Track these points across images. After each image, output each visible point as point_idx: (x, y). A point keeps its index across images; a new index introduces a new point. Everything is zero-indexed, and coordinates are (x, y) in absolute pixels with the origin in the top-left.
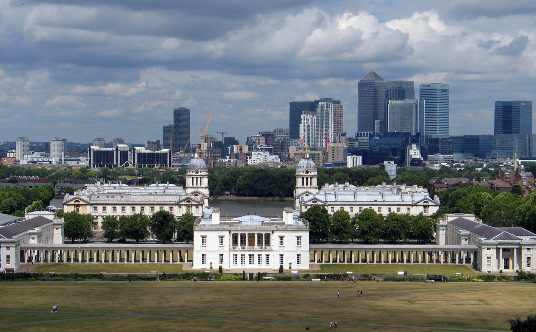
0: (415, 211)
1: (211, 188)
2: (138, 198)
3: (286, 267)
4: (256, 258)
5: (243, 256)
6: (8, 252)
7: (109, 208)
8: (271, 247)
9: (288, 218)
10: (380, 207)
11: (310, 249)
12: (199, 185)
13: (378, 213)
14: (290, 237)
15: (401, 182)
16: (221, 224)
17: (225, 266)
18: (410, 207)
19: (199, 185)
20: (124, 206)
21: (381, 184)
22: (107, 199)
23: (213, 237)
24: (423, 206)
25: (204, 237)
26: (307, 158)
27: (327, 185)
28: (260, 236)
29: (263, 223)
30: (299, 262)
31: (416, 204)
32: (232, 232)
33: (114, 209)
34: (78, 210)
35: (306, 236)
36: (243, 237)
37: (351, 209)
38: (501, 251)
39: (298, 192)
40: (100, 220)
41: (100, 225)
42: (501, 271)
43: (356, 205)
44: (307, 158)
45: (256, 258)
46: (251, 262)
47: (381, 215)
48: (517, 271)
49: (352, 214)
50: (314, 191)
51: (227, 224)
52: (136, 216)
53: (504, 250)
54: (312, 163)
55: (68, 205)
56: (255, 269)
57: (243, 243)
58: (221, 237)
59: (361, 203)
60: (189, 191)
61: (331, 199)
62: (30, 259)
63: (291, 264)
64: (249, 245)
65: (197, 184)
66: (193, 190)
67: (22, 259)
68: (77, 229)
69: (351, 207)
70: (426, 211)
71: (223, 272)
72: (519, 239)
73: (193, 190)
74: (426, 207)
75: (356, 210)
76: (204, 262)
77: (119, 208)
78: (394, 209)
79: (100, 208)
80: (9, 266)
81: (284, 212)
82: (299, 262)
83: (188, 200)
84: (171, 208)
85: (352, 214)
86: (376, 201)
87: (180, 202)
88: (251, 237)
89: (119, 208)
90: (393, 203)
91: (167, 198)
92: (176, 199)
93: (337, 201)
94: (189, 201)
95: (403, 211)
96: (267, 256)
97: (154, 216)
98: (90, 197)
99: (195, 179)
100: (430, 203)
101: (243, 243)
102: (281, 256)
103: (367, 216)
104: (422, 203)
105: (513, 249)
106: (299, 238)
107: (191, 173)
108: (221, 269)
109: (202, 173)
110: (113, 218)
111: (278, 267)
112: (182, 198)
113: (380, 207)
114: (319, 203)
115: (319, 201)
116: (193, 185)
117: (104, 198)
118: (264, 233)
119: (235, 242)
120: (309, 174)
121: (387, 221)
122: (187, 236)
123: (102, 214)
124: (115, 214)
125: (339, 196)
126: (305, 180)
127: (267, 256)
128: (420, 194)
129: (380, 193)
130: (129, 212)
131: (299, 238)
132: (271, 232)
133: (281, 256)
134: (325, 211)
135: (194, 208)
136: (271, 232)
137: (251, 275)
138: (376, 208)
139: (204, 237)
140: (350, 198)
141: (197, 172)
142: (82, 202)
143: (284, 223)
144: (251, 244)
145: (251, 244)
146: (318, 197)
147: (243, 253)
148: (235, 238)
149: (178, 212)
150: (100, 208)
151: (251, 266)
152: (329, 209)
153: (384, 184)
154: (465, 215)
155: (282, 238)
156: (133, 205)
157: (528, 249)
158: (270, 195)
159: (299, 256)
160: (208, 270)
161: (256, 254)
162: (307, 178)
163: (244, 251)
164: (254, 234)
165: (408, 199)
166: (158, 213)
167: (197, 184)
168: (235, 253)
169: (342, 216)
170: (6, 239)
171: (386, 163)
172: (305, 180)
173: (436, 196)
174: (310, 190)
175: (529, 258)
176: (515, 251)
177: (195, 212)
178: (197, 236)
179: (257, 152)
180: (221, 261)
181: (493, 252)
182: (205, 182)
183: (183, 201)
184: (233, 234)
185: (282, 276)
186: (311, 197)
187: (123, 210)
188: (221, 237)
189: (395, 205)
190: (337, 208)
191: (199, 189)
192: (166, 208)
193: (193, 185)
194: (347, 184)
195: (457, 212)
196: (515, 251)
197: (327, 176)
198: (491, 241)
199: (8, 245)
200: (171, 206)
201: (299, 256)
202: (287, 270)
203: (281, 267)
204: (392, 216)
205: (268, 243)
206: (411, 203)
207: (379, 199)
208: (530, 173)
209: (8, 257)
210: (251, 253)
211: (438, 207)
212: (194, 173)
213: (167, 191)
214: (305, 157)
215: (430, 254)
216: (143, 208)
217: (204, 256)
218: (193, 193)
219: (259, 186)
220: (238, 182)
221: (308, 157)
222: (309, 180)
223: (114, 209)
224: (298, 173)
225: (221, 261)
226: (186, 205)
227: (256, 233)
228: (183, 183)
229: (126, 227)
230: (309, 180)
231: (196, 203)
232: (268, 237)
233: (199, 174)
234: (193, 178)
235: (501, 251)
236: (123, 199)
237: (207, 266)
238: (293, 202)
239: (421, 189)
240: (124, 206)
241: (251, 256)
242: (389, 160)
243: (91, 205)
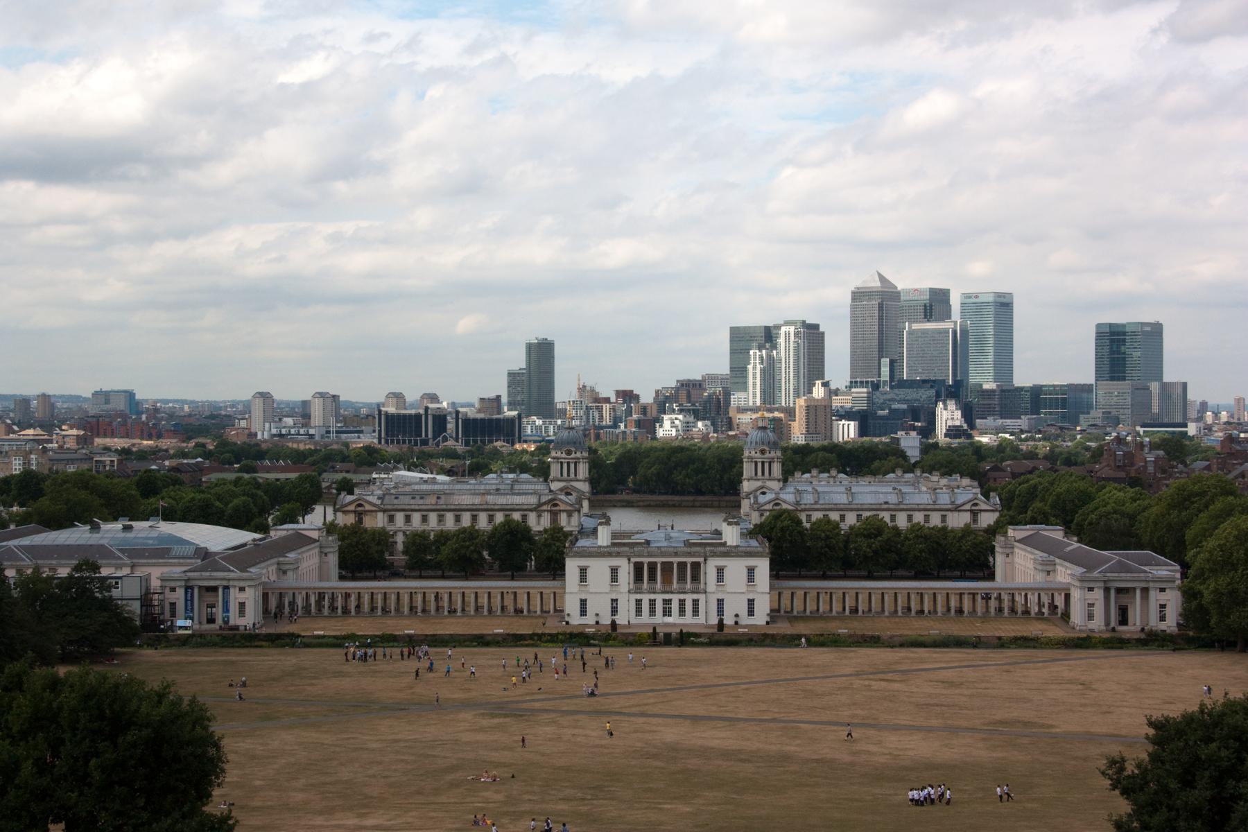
0: (958, 521)
1: (592, 481)
2: (467, 500)
3: (729, 620)
4: (675, 606)
5: (652, 603)
6: (242, 597)
7: (416, 517)
8: (702, 586)
9: (731, 535)
11: (772, 588)
12: (572, 475)
13: (890, 525)
14: (736, 569)
15: (930, 469)
16: (613, 545)
17: (621, 620)
19: (572, 475)
20: (441, 513)
21: (894, 472)
22: (412, 502)
23: (599, 569)
24: (971, 511)
25: (583, 571)
27: (797, 474)
28: (682, 566)
29: (687, 543)
30: (751, 612)
31: (957, 509)
32: (633, 560)
33: (425, 519)
34: (360, 521)
35: (763, 566)
36: (652, 567)
37: (843, 518)
38: (1113, 592)
39: (746, 486)
40: (400, 539)
41: (400, 547)
42: (1113, 630)
43: (852, 510)
45: (675, 606)
46: (667, 612)
47: (896, 528)
48: (1143, 630)
49: (844, 527)
50: (775, 485)
51: (624, 545)
52: (464, 530)
53: (1119, 591)
55: (345, 512)
56: (674, 625)
57: (652, 578)
58: (614, 571)
61: (808, 499)
62: (280, 606)
63: (737, 616)
64: (663, 582)
66: (562, 484)
67: (266, 611)
68: (362, 555)
70: (975, 520)
71: (619, 631)
72: (1145, 572)
73: (562, 484)
74: (975, 514)
75: (851, 519)
76: (583, 612)
77: (433, 517)
78: (919, 517)
79: (400, 517)
80: (241, 622)
82: (751, 612)
83: (553, 503)
84: (524, 517)
85: (844, 527)
87: (540, 505)
88: (667, 567)
89: (433, 517)
91: (518, 500)
92: (533, 500)
93: (816, 503)
94: (556, 505)
95: (935, 520)
96: (696, 602)
97: (495, 529)
98: (381, 498)
99: (565, 466)
100: (983, 506)
101: (652, 578)
102: (720, 603)
103: (872, 529)
104: (968, 507)
105: (1134, 589)
106: (751, 571)
107: (559, 454)
108: (613, 623)
109: (579, 455)
110: (423, 536)
111: (714, 620)
112: (544, 499)
114: (785, 506)
115: (785, 502)
117: (405, 501)
118: (689, 560)
119: (638, 577)
120: (767, 455)
121: (907, 538)
122: (554, 568)
123: (404, 528)
124: (425, 527)
126: (760, 465)
127: (696, 602)
128: (967, 490)
129: (894, 489)
130: (450, 523)
131: (751, 571)
132: (701, 560)
133: (720, 603)
134: (799, 522)
135: (564, 516)
136: (701, 560)
137: (667, 636)
138: (886, 516)
139: (583, 571)
140: (842, 499)
141: (569, 453)
142: (368, 507)
144: (667, 580)
145: (667, 580)
146: (782, 496)
147: (652, 596)
148: (638, 568)
149: (538, 524)
150: (400, 517)
151: (668, 620)
152: (803, 517)
153: (899, 472)
155: (720, 571)
156: (458, 511)
157: (1163, 590)
159: (751, 603)
160: (591, 626)
161: (675, 598)
162: (763, 463)
164: (672, 563)
165: (944, 499)
166: (503, 525)
168: (638, 596)
169: (827, 529)
170: (238, 574)
171: (900, 434)
172: (760, 465)
173: (992, 494)
174: (769, 484)
175: (1163, 606)
176: (1138, 592)
177: (568, 524)
178: (572, 566)
179: (674, 416)
180: (614, 611)
181: (1098, 595)
182: (583, 470)
183: (545, 503)
184: (636, 564)
185: (722, 637)
186: (769, 496)
187: (440, 521)
188: (614, 571)
189: (919, 510)
190: (817, 516)
192: (517, 516)
194: (833, 472)
195: (1034, 521)
196: (1138, 592)
197: (799, 461)
198: (1095, 574)
199: (242, 584)
200: (525, 510)
201: (751, 603)
202: (730, 627)
203: (721, 621)
204: (916, 529)
205: (696, 578)
207: (893, 499)
208: (1161, 453)
209: (242, 605)
210: (667, 597)
211: (997, 514)
212: (564, 455)
213: (517, 487)
215: (987, 598)
216: (474, 518)
217: (583, 603)
218: (561, 490)
219: (678, 477)
220: (641, 471)
222: (767, 466)
223: (425, 519)
224: (746, 453)
225: (614, 611)
226: (550, 511)
227: (676, 560)
228: (543, 472)
229: (446, 550)
230: (767, 466)
231: (569, 508)
232: (696, 566)
235: (1113, 592)
236: (441, 501)
237: (590, 620)
238: (739, 506)
239: (966, 481)
240: (441, 513)
241: (667, 602)
243: (384, 511)
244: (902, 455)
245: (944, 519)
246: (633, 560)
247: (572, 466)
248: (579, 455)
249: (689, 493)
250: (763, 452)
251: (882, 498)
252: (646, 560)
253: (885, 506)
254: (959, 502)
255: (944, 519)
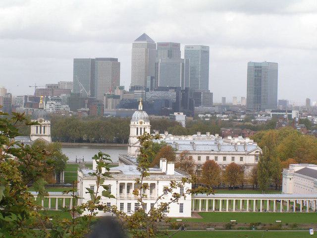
10: (216, 156)
12: (42, 133)
18: (244, 157)
19: (42, 133)
26: (140, 111)
30: (181, 211)
31: (248, 154)
43: (196, 154)
44: (140, 111)
54: (145, 114)
57: (128, 192)
59: (199, 152)
60: (34, 138)
65: (41, 133)
69: (224, 156)
81: (161, 161)
82: (181, 211)
86: (213, 151)
90: (228, 153)
95: (237, 161)
99: (39, 128)
104: (253, 153)
109: (46, 122)
113: (216, 156)
116: (37, 133)
120: (143, 124)
125: (180, 146)
132: (156, 182)
143: (164, 174)
148: (122, 186)
152: (195, 158)
153: (199, 134)
154: (310, 165)
158: (80, 140)
163: (130, 200)
165: (241, 150)
167: (41, 133)
169: (210, 166)
171: (176, 114)
182: (48, 131)
189: (229, 154)
191: (44, 137)
193: (37, 133)
206: (245, 153)
214: (139, 109)
221: (142, 109)
224: (132, 123)
233: (43, 123)
234: (37, 127)
238: (125, 148)
242: (178, 111)
244: (179, 124)
245: (241, 159)
246: (120, 182)
247: (43, 128)
248: (46, 122)
249: (77, 141)
250: (141, 123)
251: (211, 148)
252: (126, 182)
253: (213, 152)
254: (249, 150)
255: (241, 159)
